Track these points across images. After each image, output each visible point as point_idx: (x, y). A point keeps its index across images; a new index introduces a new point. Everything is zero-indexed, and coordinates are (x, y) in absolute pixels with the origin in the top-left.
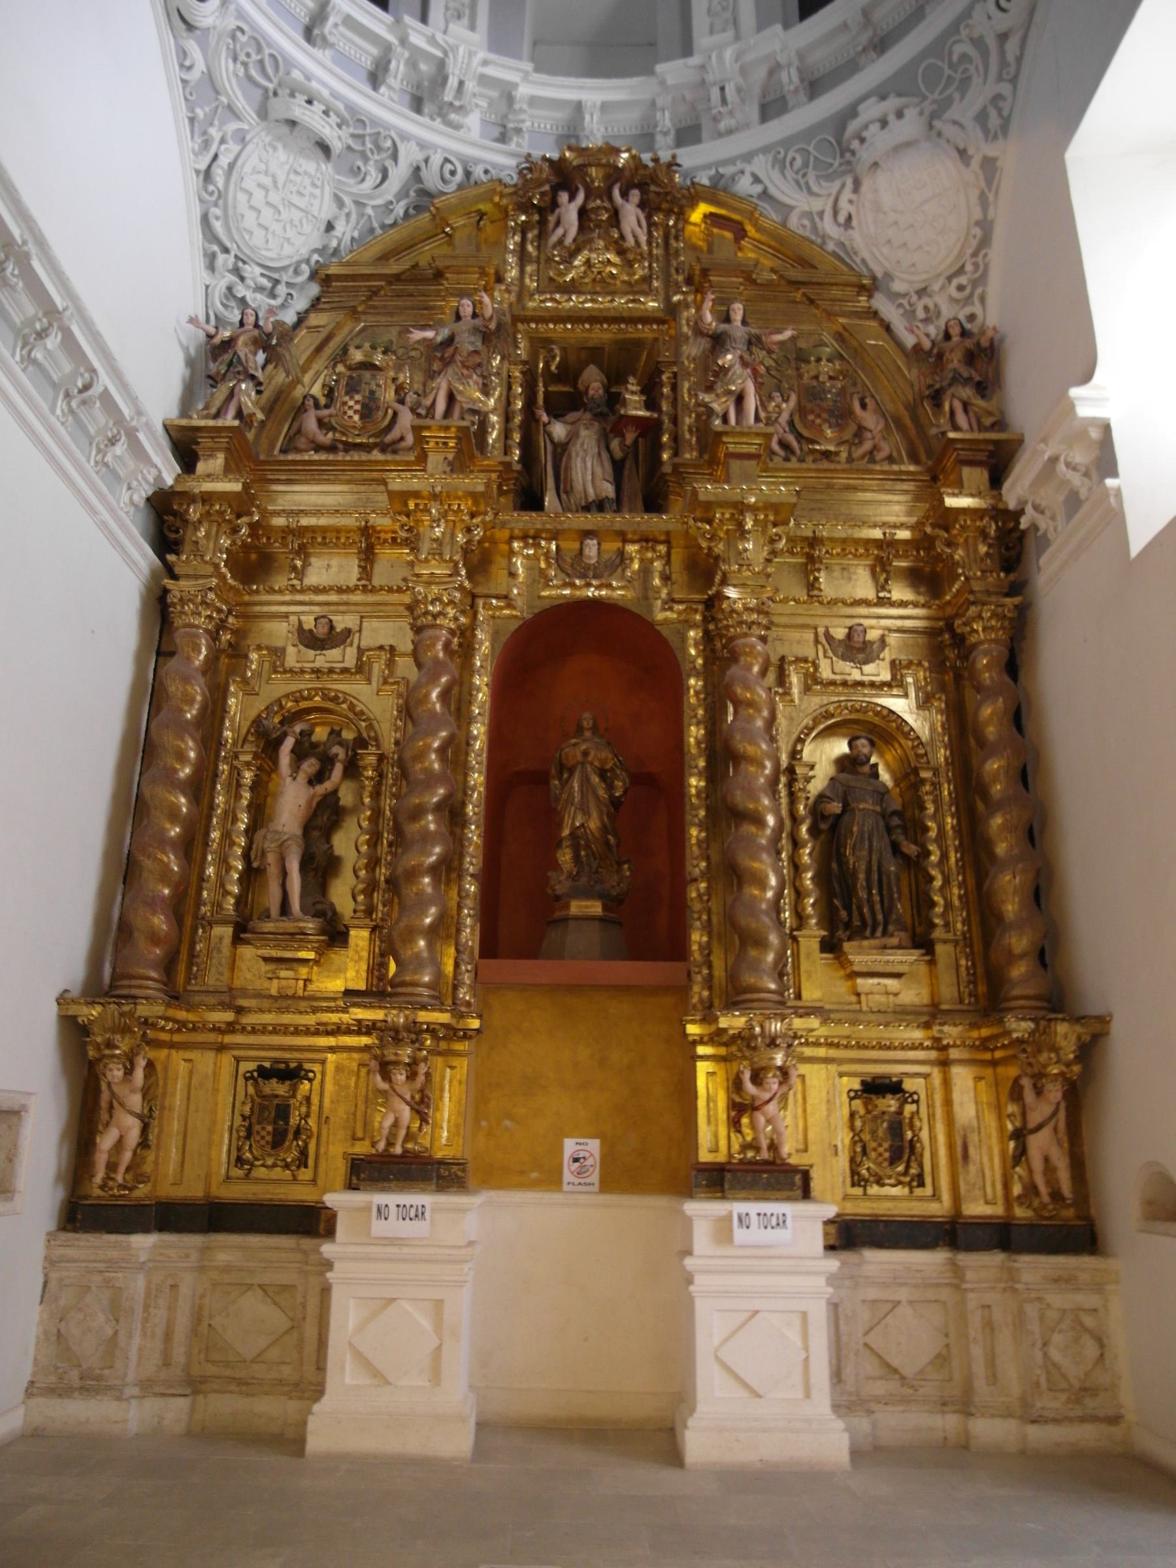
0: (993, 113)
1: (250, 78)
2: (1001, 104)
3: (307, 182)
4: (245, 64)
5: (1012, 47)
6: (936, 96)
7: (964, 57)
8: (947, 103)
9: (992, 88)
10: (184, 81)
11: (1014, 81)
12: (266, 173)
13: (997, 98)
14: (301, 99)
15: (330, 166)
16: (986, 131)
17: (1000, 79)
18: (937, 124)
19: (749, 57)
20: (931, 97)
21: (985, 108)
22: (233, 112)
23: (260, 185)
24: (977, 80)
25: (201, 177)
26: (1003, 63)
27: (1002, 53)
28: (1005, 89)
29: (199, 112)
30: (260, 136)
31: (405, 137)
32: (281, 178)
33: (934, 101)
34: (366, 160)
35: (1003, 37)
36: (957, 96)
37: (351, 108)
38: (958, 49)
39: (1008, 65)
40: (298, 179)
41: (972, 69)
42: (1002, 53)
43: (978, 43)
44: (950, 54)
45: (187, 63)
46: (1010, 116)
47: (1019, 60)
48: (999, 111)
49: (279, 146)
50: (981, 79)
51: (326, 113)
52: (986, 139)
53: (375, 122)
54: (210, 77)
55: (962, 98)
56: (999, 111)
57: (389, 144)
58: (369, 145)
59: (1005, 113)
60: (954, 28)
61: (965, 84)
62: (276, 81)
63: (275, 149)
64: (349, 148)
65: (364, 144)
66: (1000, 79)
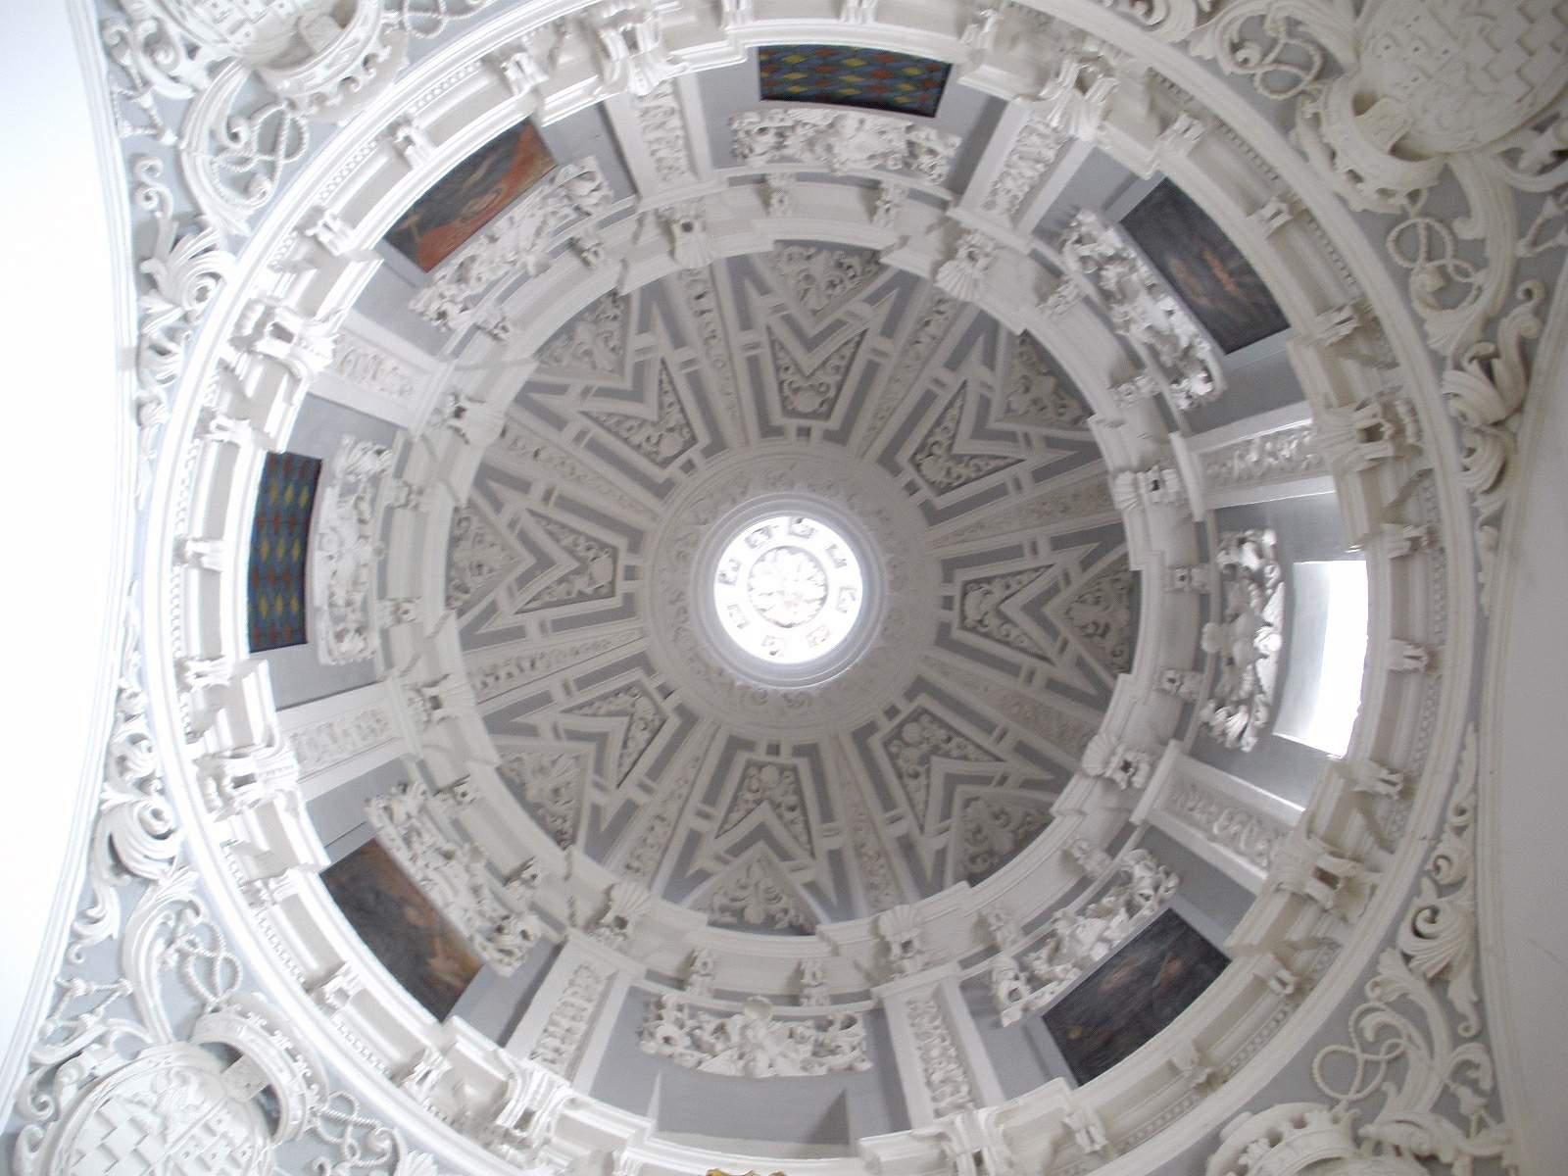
0: (1464, 1093)
1: (183, 977)
2: (1472, 1074)
3: (223, 1151)
4: (183, 956)
5: (1460, 991)
6: (1352, 1095)
7: (1384, 1030)
8: (1378, 1100)
9: (1446, 1059)
10: (76, 937)
11: (1481, 1035)
12: (154, 1109)
13: (1462, 1071)
14: (255, 1021)
15: (271, 1147)
16: (1462, 1122)
17: (1457, 1041)
18: (1369, 1130)
19: (1019, 1120)
20: (1344, 1099)
21: (1446, 1088)
22: (133, 1005)
23: (133, 1121)
24: (1416, 1056)
25: (38, 1075)
26: (1453, 1016)
27: (1447, 1006)
28: (1473, 1052)
29: (80, 987)
30: (163, 1054)
31: (415, 1146)
32: (176, 1130)
33: (1352, 1104)
34: (338, 1158)
35: (1438, 982)
36: (1390, 1088)
37: (337, 1081)
38: (1369, 1024)
39: (1464, 1018)
40: (208, 1141)
41: (1403, 1041)
42: (1447, 1006)
43: (1404, 1005)
44: (1360, 1033)
45: (93, 913)
46: (1495, 1089)
47: (1479, 1006)
48: (1474, 1085)
49: (194, 1081)
50: (1424, 1052)
51: (292, 1054)
52: (1468, 1135)
53: (368, 1109)
54: (117, 949)
55: (1400, 1089)
56: (1474, 1085)
57: (386, 1145)
58: (350, 1139)
59: (1486, 1085)
60: (1357, 994)
61: (1397, 1065)
62: (224, 997)
63: (185, 1081)
64: (313, 1132)
65: (342, 1135)
66: (1457, 1041)
